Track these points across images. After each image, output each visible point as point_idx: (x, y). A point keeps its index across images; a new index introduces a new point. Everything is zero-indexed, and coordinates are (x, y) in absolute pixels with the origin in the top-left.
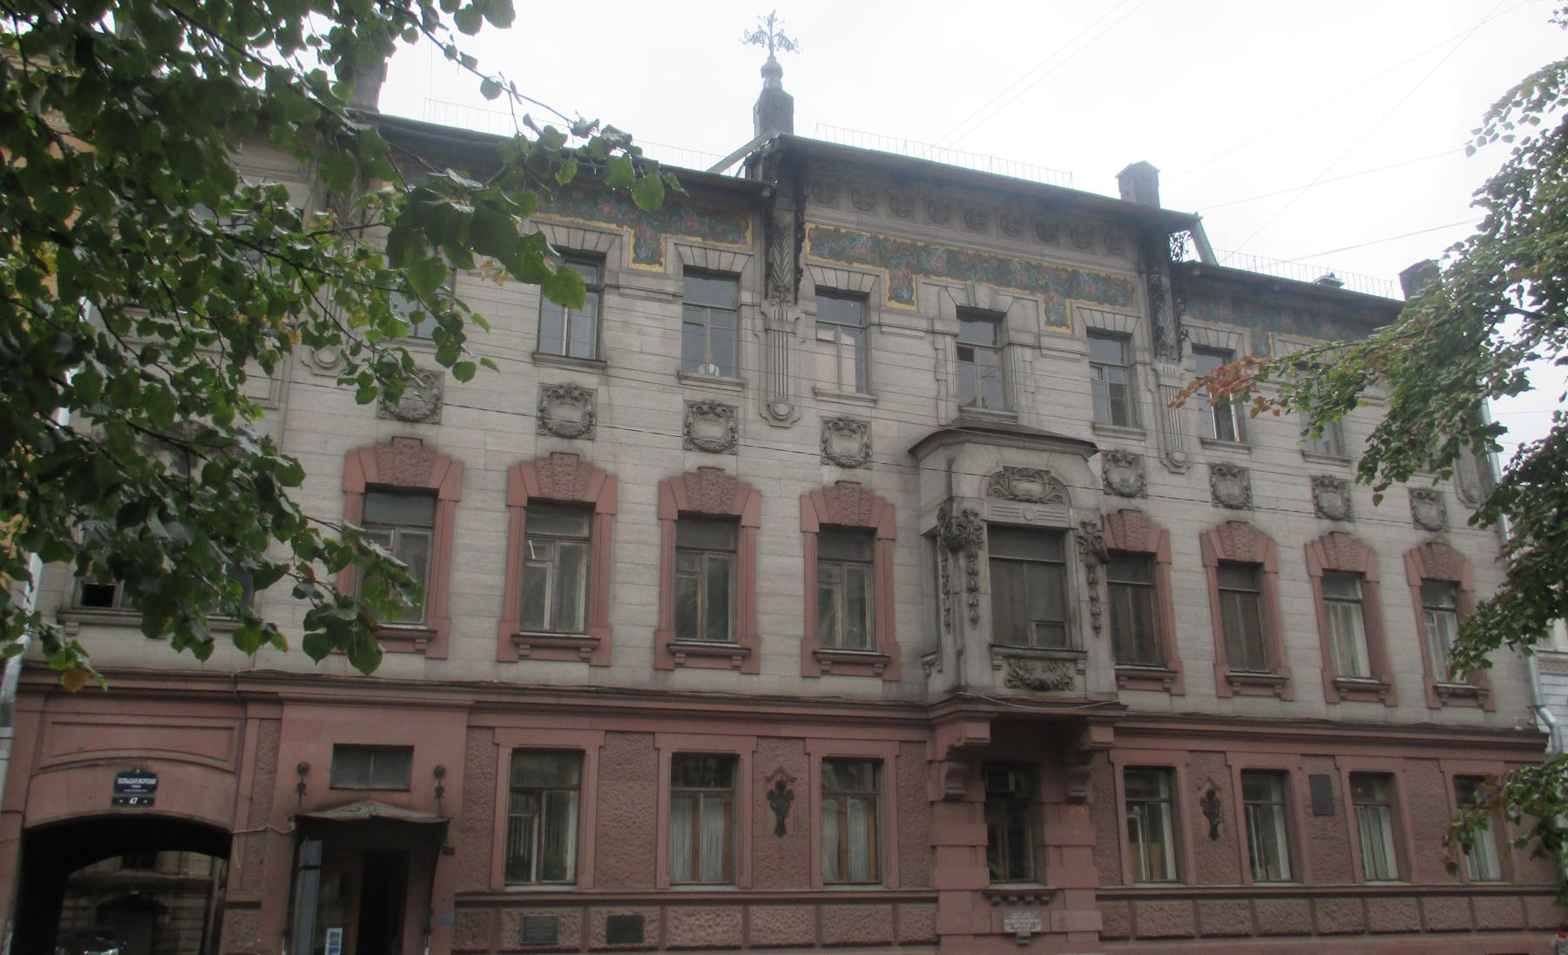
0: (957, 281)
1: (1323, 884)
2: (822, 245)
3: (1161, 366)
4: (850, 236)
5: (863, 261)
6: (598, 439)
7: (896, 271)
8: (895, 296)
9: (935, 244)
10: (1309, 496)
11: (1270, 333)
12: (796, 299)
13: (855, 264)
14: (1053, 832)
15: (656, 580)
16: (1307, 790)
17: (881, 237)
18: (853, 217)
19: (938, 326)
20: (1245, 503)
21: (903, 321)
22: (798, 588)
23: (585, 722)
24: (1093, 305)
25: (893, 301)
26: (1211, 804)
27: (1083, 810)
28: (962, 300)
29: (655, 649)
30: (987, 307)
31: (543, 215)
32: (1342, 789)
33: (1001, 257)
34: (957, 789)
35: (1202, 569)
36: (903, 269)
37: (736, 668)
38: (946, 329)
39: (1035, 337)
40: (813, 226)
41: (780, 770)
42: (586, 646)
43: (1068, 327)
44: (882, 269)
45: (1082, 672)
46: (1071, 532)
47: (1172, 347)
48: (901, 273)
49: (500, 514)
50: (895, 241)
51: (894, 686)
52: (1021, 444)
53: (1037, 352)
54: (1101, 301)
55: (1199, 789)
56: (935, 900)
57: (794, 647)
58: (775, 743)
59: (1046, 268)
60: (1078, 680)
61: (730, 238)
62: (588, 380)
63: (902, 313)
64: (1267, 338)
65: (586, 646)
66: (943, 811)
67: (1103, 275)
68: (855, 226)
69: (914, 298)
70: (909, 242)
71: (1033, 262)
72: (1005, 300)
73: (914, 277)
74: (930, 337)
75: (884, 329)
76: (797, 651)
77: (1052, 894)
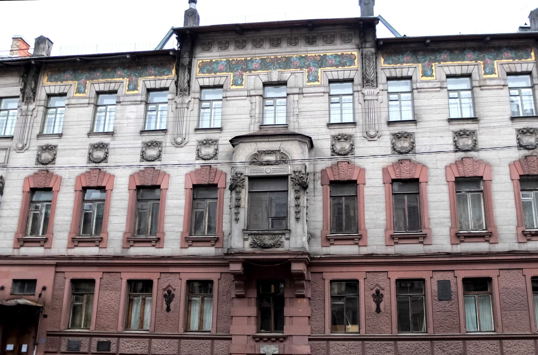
0: (265, 71)
1: (440, 334)
2: (204, 68)
3: (366, 91)
4: (217, 62)
5: (221, 71)
6: (109, 162)
7: (236, 73)
8: (235, 83)
9: (255, 57)
10: (451, 141)
11: (433, 64)
12: (189, 93)
13: (218, 74)
14: (288, 311)
15: (126, 214)
16: (435, 288)
17: (231, 60)
18: (218, 54)
19: (252, 93)
20: (412, 149)
21: (236, 93)
22: (182, 212)
23: (95, 269)
24: (334, 68)
25: (233, 86)
26: (378, 297)
27: (305, 300)
28: (265, 79)
29: (123, 241)
30: (276, 80)
31: (96, 80)
32: (458, 287)
33: (287, 56)
34: (241, 292)
35: (383, 185)
36: (240, 71)
37: (154, 246)
38: (256, 94)
39: (300, 89)
40: (201, 61)
41: (169, 286)
42: (97, 241)
43: (319, 81)
44: (230, 73)
45: (288, 239)
46: (289, 177)
47: (372, 81)
48: (238, 73)
49: (72, 194)
50: (237, 60)
51: (220, 250)
52: (267, 140)
53: (301, 96)
54: (337, 66)
55: (372, 290)
56: (231, 339)
57: (178, 236)
58: (168, 275)
59: (310, 56)
60: (286, 243)
61: (166, 73)
62: (106, 140)
63: (237, 90)
64: (432, 66)
65: (97, 241)
66: (236, 301)
67: (339, 54)
68: (219, 58)
69: (243, 83)
70: (243, 59)
71: (303, 55)
72: (286, 75)
73: (244, 73)
74: (249, 98)
75: (228, 99)
76: (180, 238)
77: (285, 338)
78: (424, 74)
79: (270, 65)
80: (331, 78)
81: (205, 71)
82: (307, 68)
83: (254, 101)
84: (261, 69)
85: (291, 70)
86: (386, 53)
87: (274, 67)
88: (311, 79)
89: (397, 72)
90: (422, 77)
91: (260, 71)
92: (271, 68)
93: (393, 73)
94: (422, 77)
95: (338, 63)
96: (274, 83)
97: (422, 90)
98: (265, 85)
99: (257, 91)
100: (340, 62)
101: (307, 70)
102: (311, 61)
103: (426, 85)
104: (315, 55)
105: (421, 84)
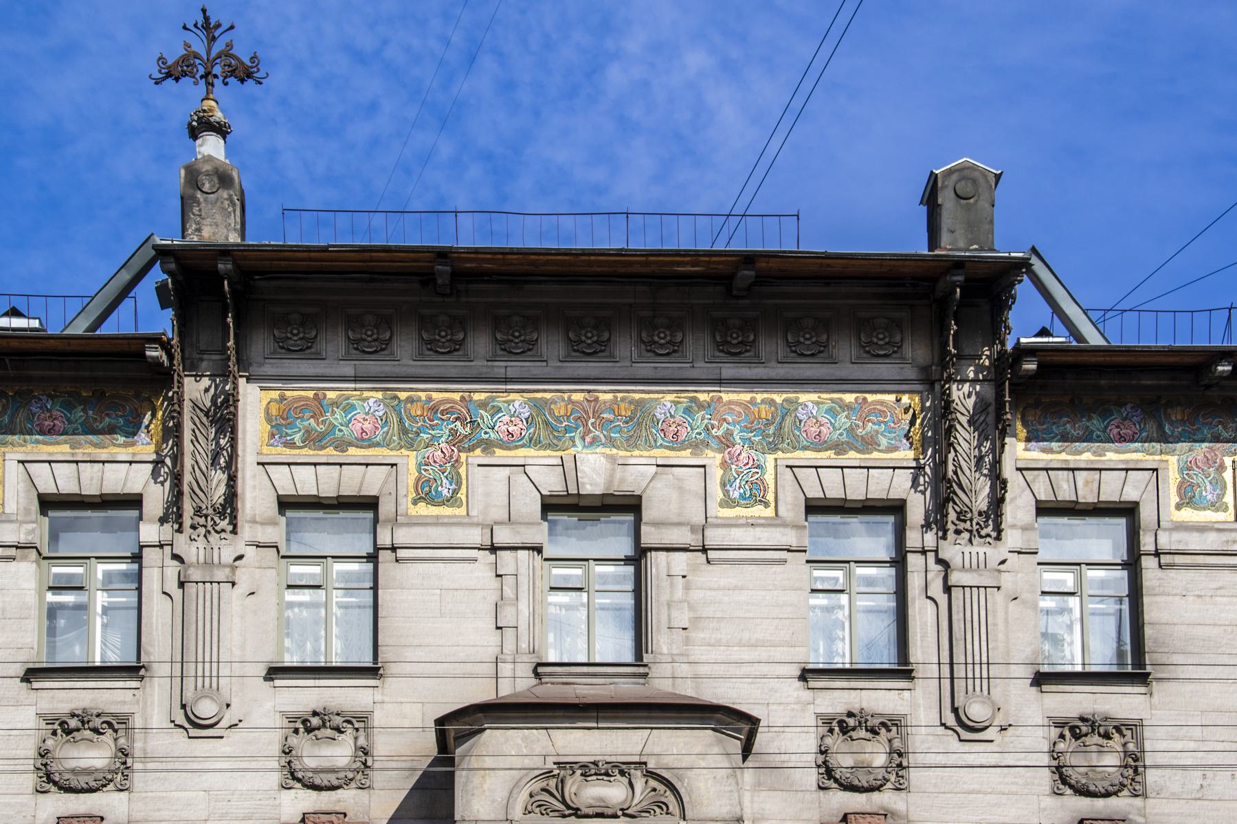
0: (548, 452)
2: (290, 425)
5: (365, 441)
8: (426, 493)
13: (352, 451)
19: (503, 536)
25: (422, 505)
28: (552, 483)
30: (598, 491)
43: (767, 505)
50: (430, 399)
59: (730, 402)
63: (437, 522)
69: (462, 495)
73: (463, 456)
78: (1188, 498)
79: (567, 430)
80: (814, 492)
81: (297, 438)
82: (721, 451)
83: (511, 570)
84: (534, 442)
85: (656, 452)
86: (1037, 405)
87: (588, 439)
88: (736, 495)
89: (1080, 484)
90: (1178, 507)
91: (531, 452)
92: (572, 439)
93: (1065, 486)
94: (1178, 507)
95: (844, 438)
96: (583, 503)
97: (1179, 559)
98: (550, 506)
99: (523, 529)
100: (851, 431)
101: (719, 456)
102: (735, 423)
103: (1194, 542)
104: (753, 401)
105: (1176, 536)
